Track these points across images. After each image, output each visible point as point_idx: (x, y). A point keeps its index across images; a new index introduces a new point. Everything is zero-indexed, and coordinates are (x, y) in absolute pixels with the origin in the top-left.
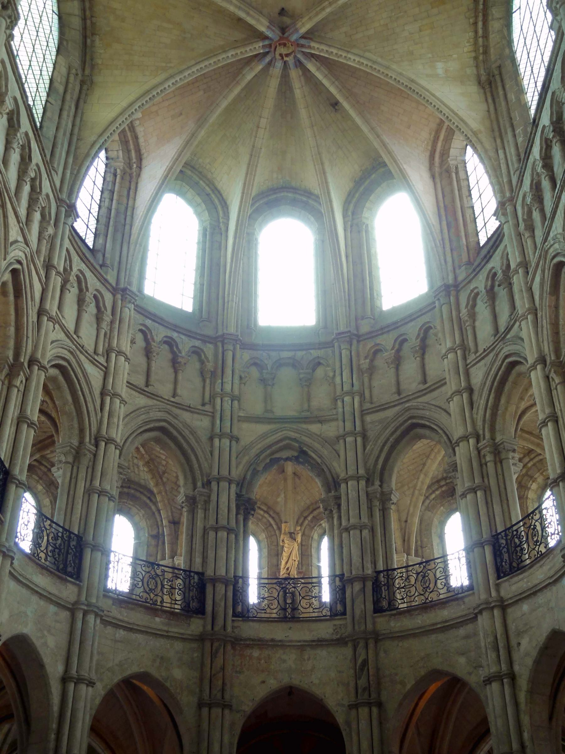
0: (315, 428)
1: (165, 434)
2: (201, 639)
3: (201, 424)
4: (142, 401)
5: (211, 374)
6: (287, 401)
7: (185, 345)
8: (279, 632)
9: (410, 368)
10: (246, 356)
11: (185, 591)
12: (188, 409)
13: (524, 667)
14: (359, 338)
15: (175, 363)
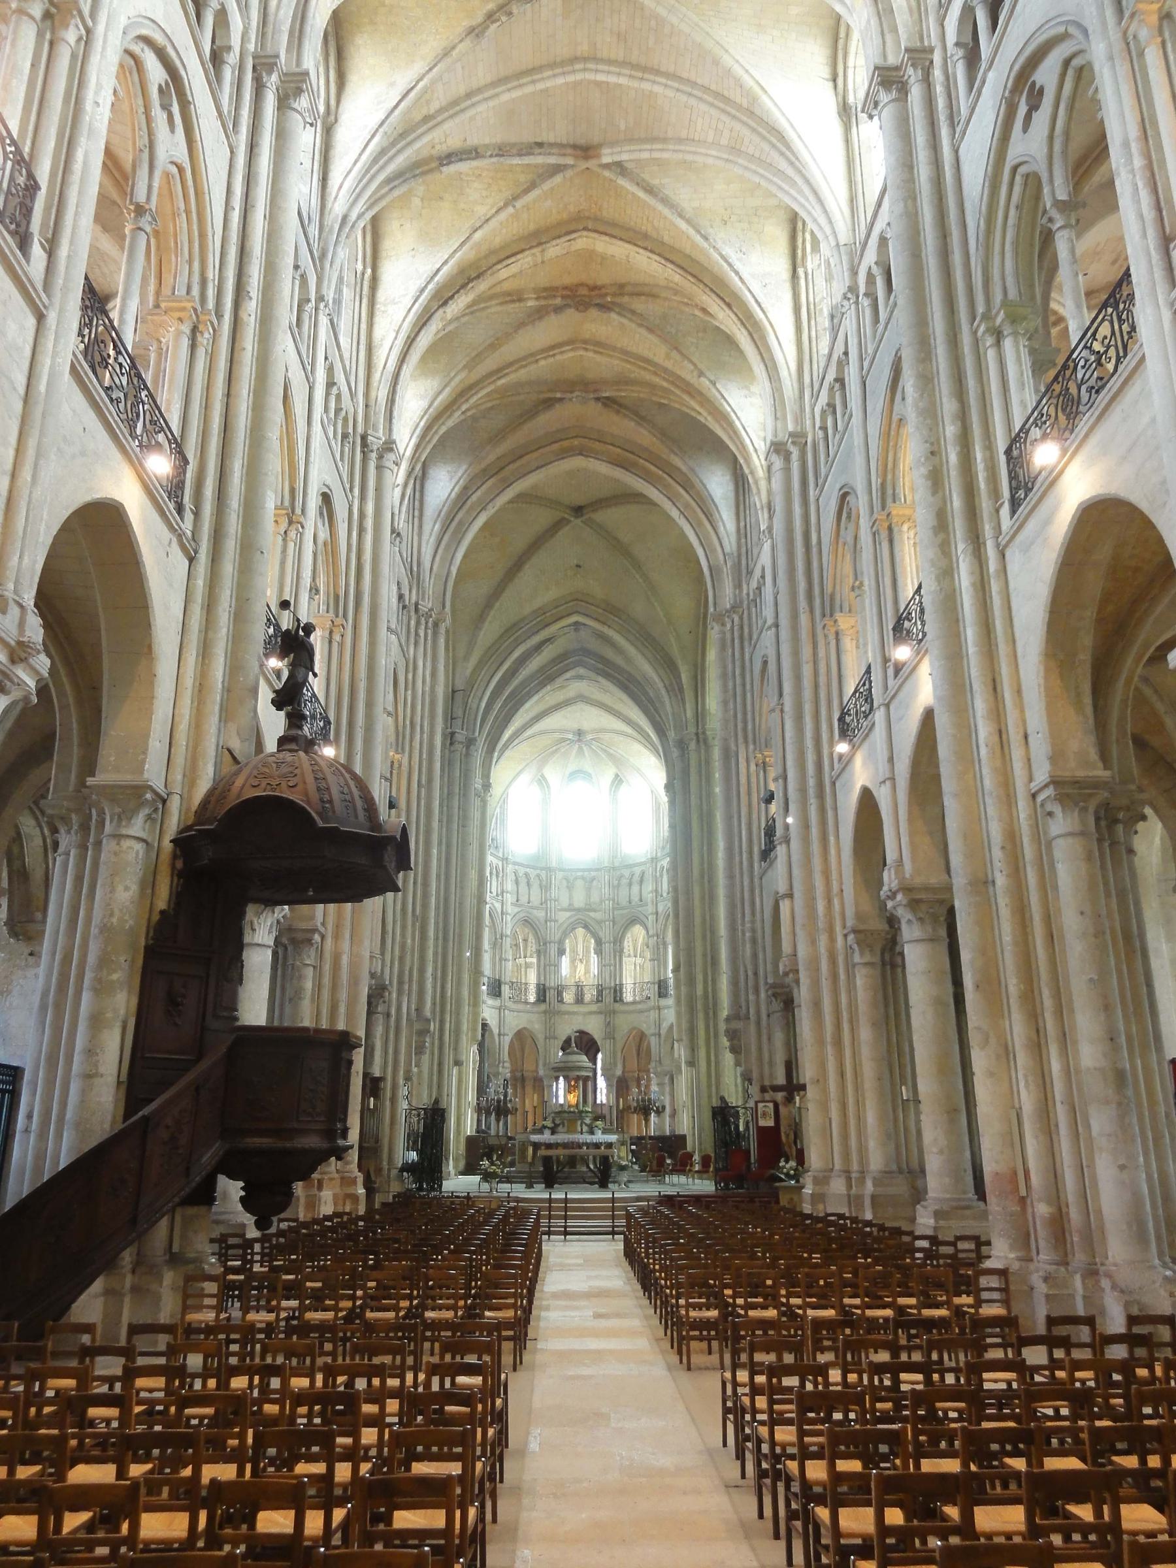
0: (592, 914)
1: (527, 922)
2: (545, 1012)
3: (541, 914)
4: (516, 910)
5: (545, 887)
6: (579, 900)
7: (533, 873)
8: (575, 1008)
9: (635, 889)
10: (560, 875)
11: (538, 994)
12: (537, 908)
13: (663, 1032)
14: (614, 868)
15: (528, 884)
